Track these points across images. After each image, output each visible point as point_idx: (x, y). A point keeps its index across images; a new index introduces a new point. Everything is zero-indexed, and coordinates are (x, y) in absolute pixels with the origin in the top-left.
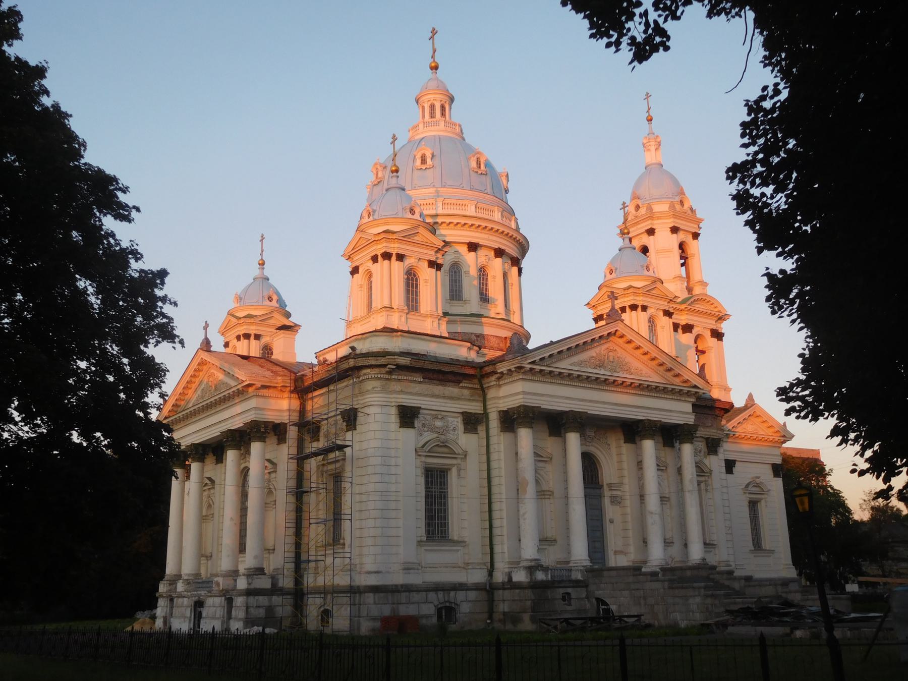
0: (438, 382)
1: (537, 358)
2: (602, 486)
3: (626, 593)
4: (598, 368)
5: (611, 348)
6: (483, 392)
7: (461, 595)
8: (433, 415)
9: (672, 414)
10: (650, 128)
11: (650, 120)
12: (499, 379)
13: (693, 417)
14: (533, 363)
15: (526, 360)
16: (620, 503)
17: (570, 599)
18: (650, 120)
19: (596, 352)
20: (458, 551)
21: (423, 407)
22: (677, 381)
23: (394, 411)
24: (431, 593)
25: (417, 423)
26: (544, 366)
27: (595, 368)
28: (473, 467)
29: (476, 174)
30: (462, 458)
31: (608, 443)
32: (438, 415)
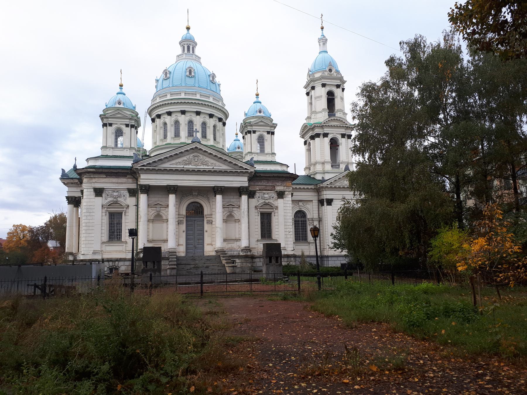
0: (114, 177)
5: (196, 155)
6: (137, 179)
7: (121, 263)
8: (113, 191)
9: (232, 182)
10: (322, 33)
11: (322, 28)
13: (248, 183)
14: (143, 166)
15: (137, 165)
16: (212, 223)
18: (322, 28)
20: (123, 245)
21: (105, 187)
23: (92, 190)
24: (106, 262)
25: (104, 195)
28: (132, 211)
29: (189, 78)
30: (126, 208)
32: (114, 190)
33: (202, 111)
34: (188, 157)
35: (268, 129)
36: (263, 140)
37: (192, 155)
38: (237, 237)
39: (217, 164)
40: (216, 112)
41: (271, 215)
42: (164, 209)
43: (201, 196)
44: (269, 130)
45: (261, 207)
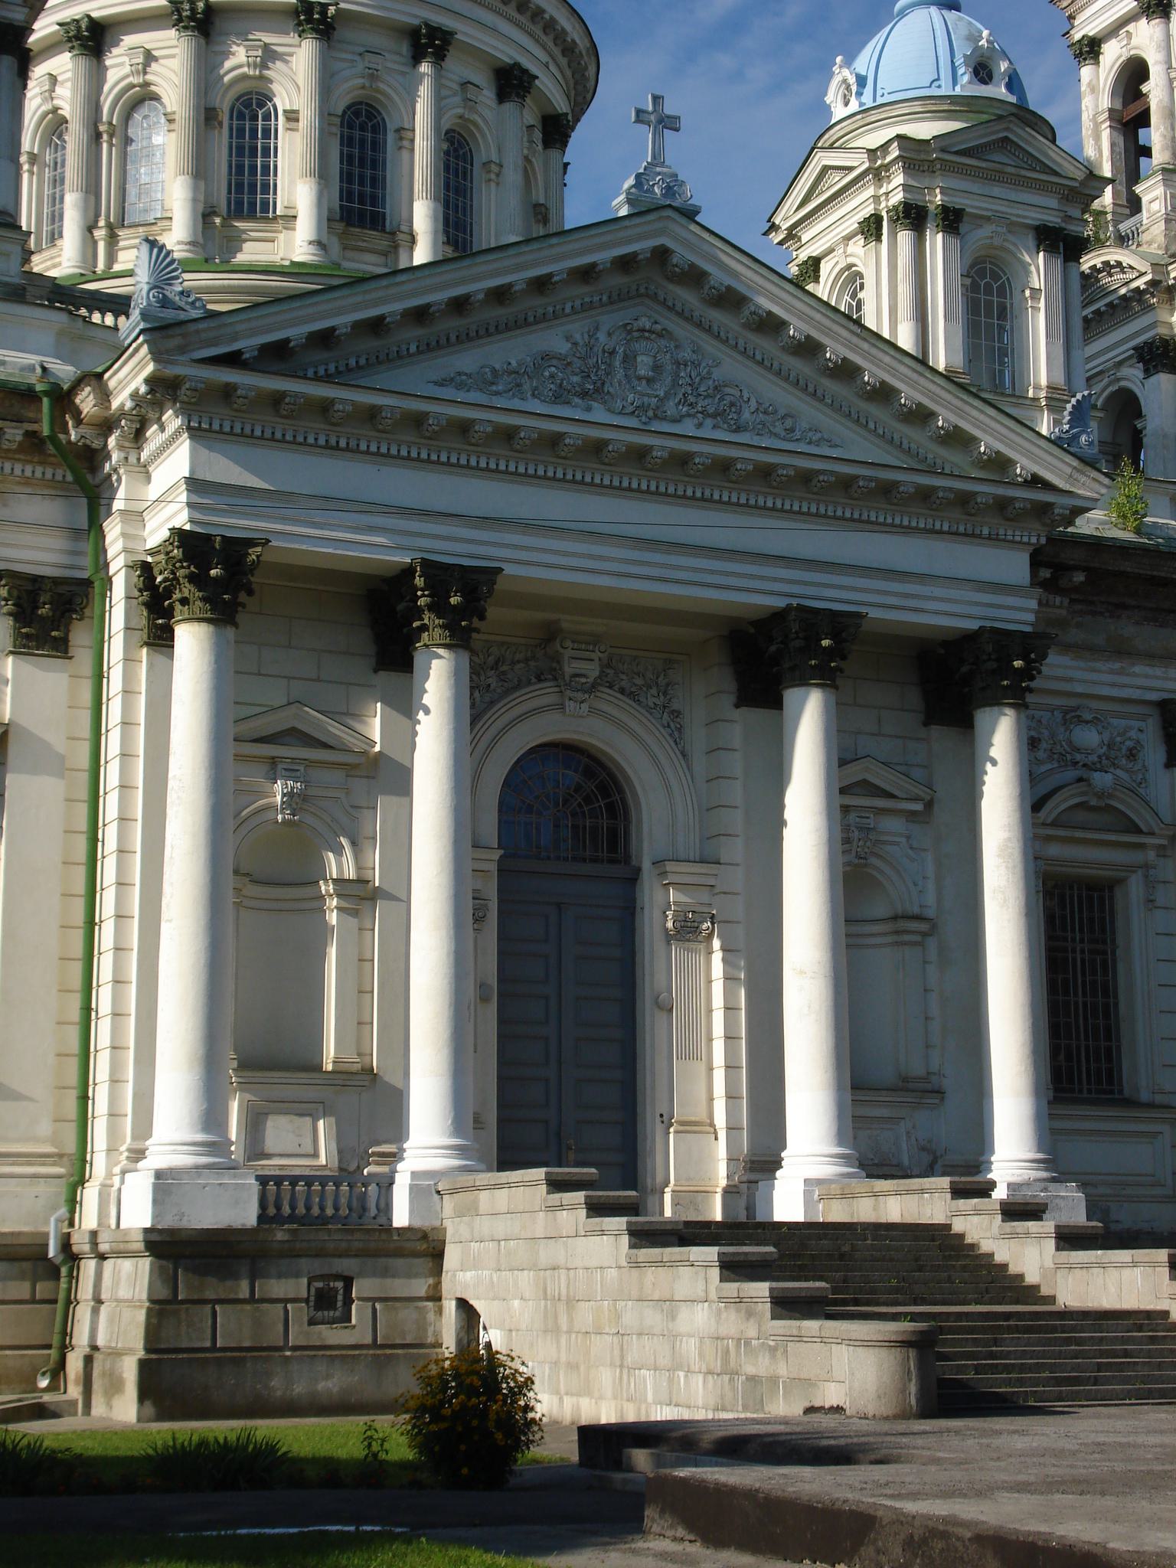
1: (248, 344)
2: (639, 870)
3: (525, 1278)
4: (577, 400)
12: (138, 436)
13: (1033, 604)
14: (233, 360)
15: (182, 350)
17: (348, 1301)
19: (568, 338)
22: (953, 458)
26: (305, 377)
27: (558, 398)
31: (675, 706)
33: (465, 32)
34: (578, 328)
35: (1045, 209)
36: (1002, 292)
37: (610, 320)
38: (917, 1069)
39: (805, 425)
40: (544, 57)
41: (1112, 898)
42: (338, 776)
43: (622, 691)
44: (1053, 219)
45: (1054, 824)
